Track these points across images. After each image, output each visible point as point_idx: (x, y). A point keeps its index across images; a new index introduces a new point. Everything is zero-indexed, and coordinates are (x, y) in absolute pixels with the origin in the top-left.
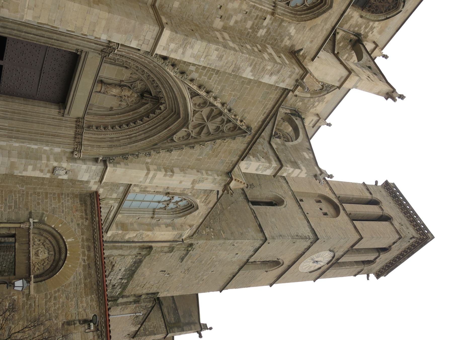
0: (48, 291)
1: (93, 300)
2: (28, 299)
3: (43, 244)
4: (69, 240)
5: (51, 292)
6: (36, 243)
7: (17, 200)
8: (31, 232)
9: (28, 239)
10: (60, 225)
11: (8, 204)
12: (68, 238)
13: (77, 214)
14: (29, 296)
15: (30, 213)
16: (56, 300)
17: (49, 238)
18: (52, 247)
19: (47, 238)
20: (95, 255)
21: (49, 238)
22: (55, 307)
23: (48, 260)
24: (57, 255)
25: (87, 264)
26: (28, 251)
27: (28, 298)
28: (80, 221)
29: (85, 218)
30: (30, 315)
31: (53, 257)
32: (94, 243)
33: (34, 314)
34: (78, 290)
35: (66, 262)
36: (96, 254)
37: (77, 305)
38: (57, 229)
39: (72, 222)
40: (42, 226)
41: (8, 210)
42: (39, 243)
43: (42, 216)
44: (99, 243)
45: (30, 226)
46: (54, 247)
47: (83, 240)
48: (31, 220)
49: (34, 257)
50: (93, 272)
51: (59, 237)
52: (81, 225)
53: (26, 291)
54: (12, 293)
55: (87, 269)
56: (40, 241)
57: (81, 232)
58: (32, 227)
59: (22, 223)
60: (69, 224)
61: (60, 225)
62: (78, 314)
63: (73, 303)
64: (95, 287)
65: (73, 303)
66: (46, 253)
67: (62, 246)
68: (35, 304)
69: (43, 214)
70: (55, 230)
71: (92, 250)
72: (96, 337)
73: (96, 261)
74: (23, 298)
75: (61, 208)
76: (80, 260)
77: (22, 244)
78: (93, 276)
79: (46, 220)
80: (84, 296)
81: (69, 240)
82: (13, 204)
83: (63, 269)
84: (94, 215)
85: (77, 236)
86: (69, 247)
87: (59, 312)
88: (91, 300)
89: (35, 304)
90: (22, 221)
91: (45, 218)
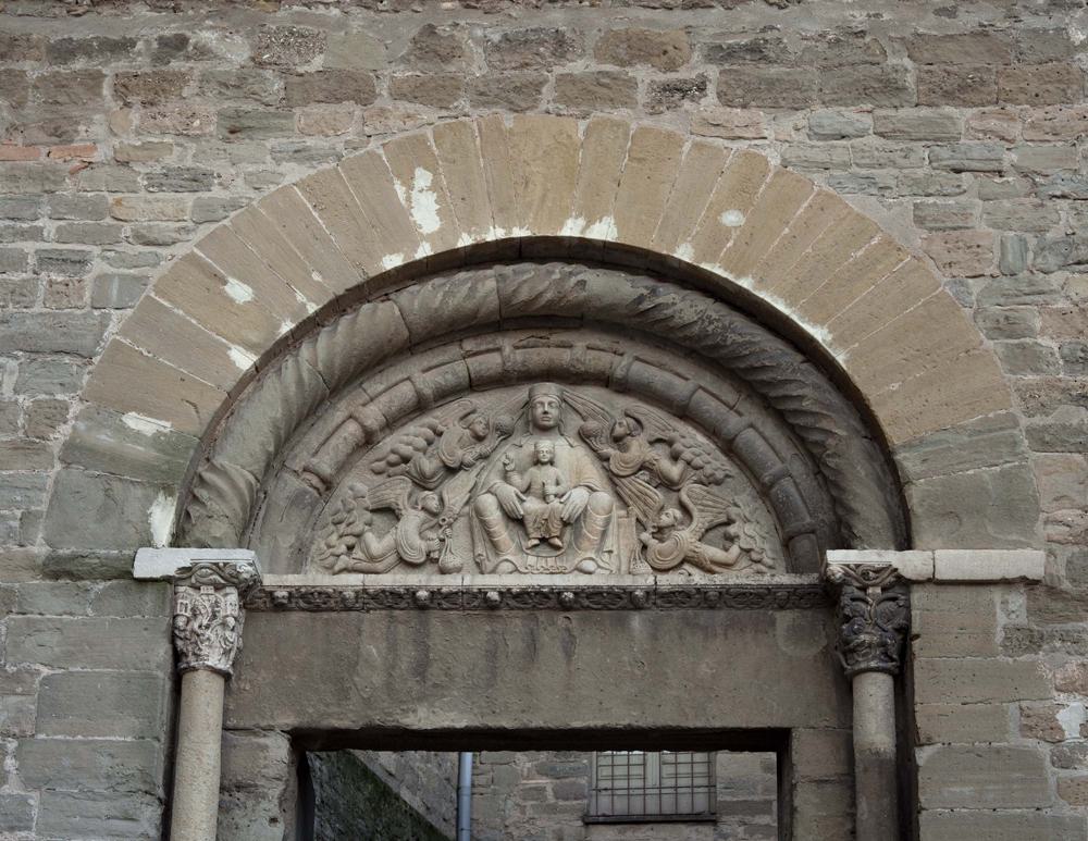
3: (422, 482)
5: (1027, 394)
8: (294, 580)
9: (375, 619)
10: (239, 291)
12: (400, 227)
14: (1052, 591)
15: (58, 570)
17: (373, 415)
19: (368, 440)
24: (581, 350)
25: (713, 72)
26: (515, 625)
28: (198, 104)
31: (590, 395)
35: (684, 253)
38: (287, 327)
39: (197, 180)
40: (240, 457)
45: (226, 577)
46: (476, 385)
48: (156, 562)
49: (586, 557)
51: (379, 319)
53: (1002, 619)
54: (1015, 740)
55: (774, 71)
57: (333, 107)
58: (242, 559)
59: (177, 656)
60: (235, 205)
61: (239, 291)
66: (546, 444)
67: (483, 288)
69: (74, 452)
75: (16, 277)
76: (667, 122)
77: (421, 669)
83: (761, 282)
85: (373, 145)
86: (503, 213)
90: (163, 651)
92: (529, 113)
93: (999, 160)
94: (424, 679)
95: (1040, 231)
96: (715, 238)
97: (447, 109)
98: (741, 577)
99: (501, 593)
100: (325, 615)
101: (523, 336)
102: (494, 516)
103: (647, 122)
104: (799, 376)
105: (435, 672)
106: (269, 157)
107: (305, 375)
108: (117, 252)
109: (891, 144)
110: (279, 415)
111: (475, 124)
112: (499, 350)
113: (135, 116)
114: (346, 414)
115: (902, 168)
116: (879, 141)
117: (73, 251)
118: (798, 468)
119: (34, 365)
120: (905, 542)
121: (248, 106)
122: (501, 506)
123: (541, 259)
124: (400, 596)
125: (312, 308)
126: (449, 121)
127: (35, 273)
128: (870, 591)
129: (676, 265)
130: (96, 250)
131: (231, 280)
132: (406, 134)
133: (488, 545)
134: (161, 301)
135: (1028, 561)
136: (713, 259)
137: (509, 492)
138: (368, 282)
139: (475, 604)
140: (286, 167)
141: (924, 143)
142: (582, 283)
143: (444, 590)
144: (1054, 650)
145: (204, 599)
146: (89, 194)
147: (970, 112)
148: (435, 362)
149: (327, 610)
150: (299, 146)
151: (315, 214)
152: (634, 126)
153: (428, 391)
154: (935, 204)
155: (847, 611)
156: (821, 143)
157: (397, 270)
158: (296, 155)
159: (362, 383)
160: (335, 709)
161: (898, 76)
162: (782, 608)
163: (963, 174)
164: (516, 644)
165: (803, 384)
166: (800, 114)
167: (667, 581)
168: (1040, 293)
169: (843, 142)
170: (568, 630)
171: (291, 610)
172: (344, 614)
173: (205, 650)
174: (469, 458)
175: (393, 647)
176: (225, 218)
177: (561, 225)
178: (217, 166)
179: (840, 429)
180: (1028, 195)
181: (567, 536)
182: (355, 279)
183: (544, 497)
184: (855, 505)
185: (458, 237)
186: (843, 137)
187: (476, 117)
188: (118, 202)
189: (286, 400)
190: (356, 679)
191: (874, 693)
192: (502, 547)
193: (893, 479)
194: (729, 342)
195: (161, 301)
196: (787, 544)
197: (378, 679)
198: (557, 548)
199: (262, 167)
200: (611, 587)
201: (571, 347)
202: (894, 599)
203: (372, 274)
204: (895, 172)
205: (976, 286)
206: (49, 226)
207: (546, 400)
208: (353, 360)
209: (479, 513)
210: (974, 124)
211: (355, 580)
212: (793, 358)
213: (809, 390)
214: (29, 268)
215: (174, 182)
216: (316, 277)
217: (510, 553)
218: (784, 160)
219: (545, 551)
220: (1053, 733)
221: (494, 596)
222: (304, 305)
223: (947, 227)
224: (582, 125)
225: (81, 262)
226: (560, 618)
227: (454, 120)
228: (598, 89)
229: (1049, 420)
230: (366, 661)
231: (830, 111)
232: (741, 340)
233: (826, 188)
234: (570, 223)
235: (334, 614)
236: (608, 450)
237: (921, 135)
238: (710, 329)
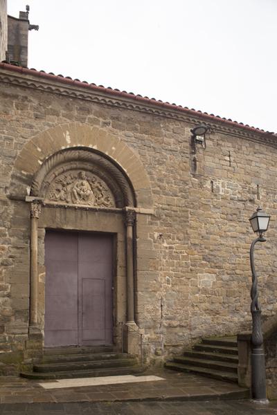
2: (159, 218)
4: (68, 140)
9: (58, 210)
13: (13, 113)
14: (154, 216)
15: (12, 198)
16: (163, 180)
17: (57, 173)
18: (70, 172)
19: (56, 176)
20: (98, 103)
22: (172, 183)
23: (93, 182)
24: (88, 166)
25: (111, 121)
29: (23, 101)
30: (179, 217)
31: (89, 173)
32: (75, 98)
34: (152, 145)
35: (107, 153)
36: (96, 100)
37: (171, 150)
43: (20, 179)
44: (80, 89)
46: (71, 169)
47: (70, 117)
48: (29, 199)
49: (89, 202)
50: (124, 115)
51: (60, 157)
52: (39, 112)
54: (149, 238)
55: (120, 123)
56: (59, 191)
59: (31, 215)
62: (184, 153)
63: (168, 156)
64: (149, 118)
65: (168, 156)
67: (76, 154)
71: (87, 105)
72: (211, 136)
73: (108, 105)
74: (157, 224)
76: (104, 129)
77: (65, 219)
78: (132, 117)
79: (28, 173)
81: (68, 140)
84: (21, 81)
86: (80, 142)
88: (168, 130)
91: (24, 175)
96: (111, 153)
102: (76, 194)
113: (20, 111)
118: (119, 190)
120: (135, 206)
121: (39, 113)
135: (151, 211)
140: (46, 127)
145: (36, 205)
147: (147, 136)
164: (79, 216)
167: (102, 207)
175: (61, 214)
178: (34, 124)
179: (127, 186)
187: (76, 122)
191: (130, 229)
193: (134, 196)
196: (116, 203)
209: (73, 192)
211: (55, 203)
212: (120, 173)
213: (123, 179)
217: (78, 200)
220: (152, 236)
225: (12, 140)
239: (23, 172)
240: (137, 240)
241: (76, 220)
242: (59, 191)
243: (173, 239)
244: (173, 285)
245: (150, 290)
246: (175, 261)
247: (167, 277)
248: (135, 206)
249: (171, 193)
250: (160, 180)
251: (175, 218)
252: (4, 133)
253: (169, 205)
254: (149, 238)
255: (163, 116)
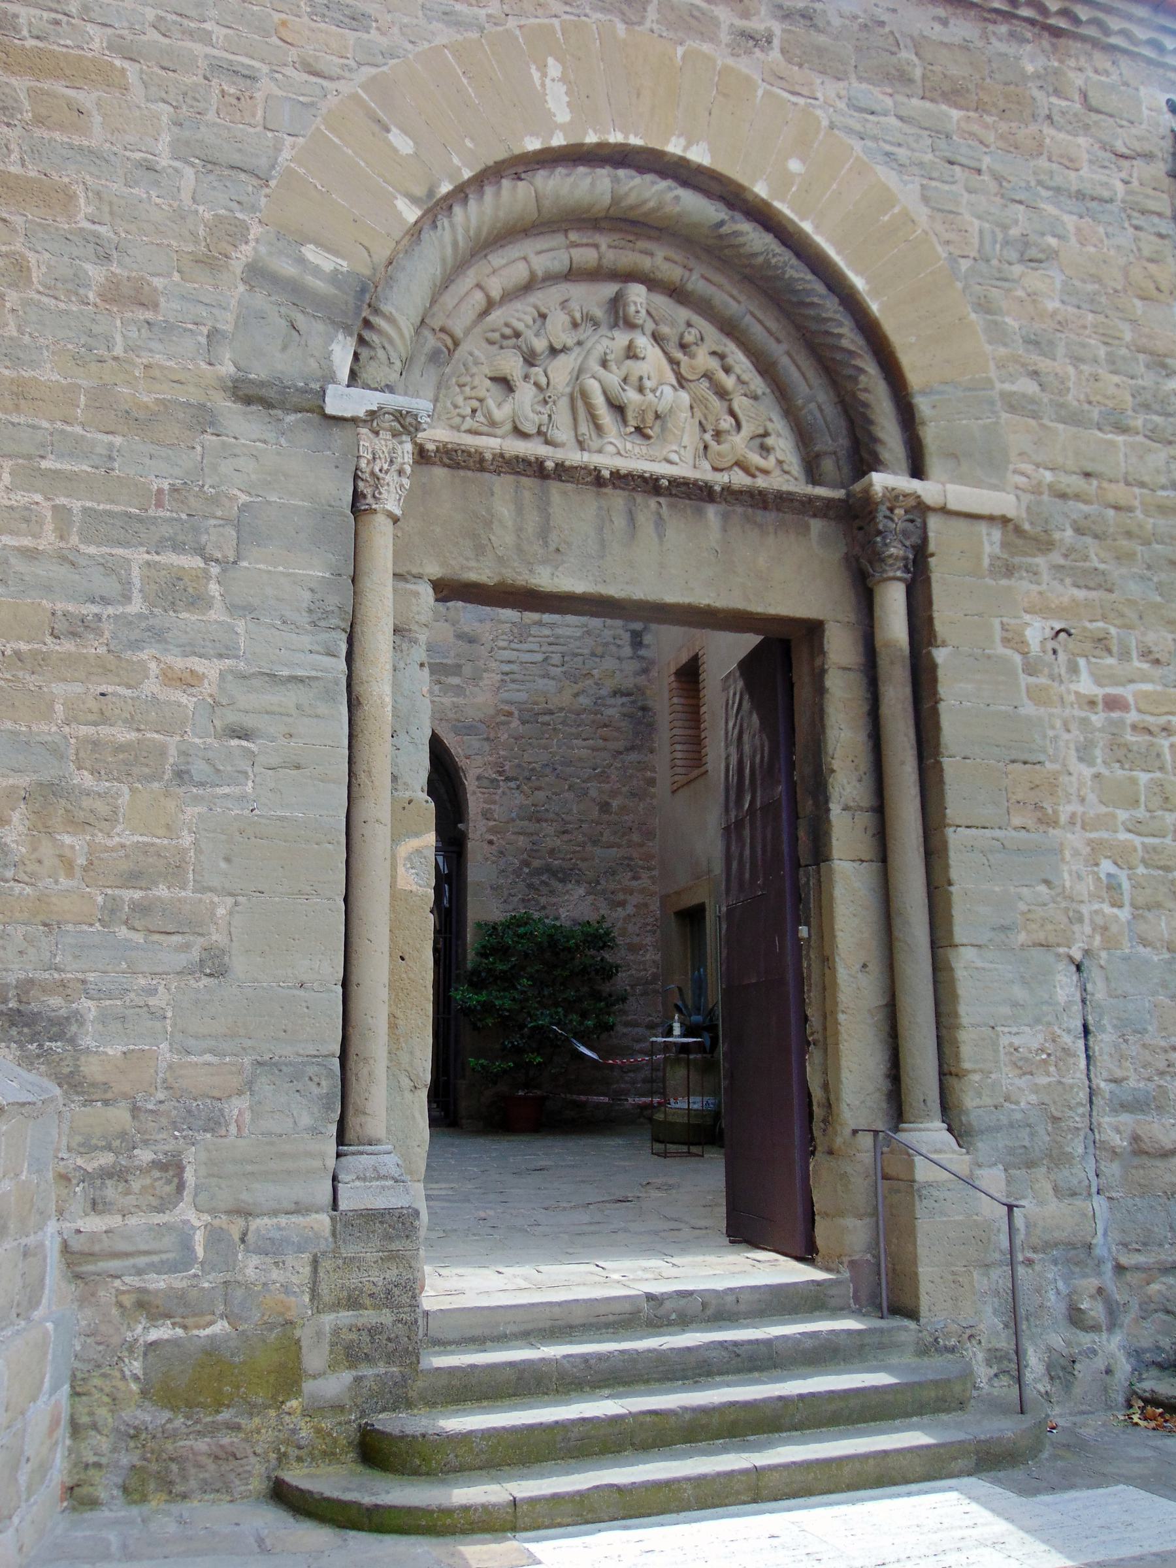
0: (989, 381)
1: (1056, 72)
2: (1044, 544)
6: (531, 415)
7: (76, 505)
10: (402, 144)
11: (136, 606)
14: (1018, 531)
21: (496, 294)
25: (777, 27)
26: (617, 499)
27: (1036, 539)
30: (1146, 543)
31: (661, 301)
33: (1139, 514)
35: (761, 190)
37: (1080, 196)
38: (445, 188)
41: (217, 614)
42: (526, 394)
43: (295, 292)
46: (573, 274)
49: (670, 449)
55: (822, 39)
61: (402, 144)
65: (1070, 221)
68: (1077, 497)
70: (446, 204)
76: (744, 65)
77: (544, 533)
80: (1033, 128)
82: (139, 556)
83: (817, 227)
85: (512, 23)
87: (1128, 336)
88: (1057, 92)
89: (1077, 497)
91: (316, 271)
92: (637, 28)
93: (979, 160)
94: (546, 545)
95: (1005, 228)
97: (571, 5)
98: (776, 482)
99: (612, 473)
100: (462, 473)
101: (616, 236)
102: (599, 401)
103: (730, 61)
104: (838, 316)
105: (554, 537)
106: (420, 13)
107: (460, 238)
108: (284, 75)
109: (906, 128)
110: (438, 273)
111: (594, 27)
112: (596, 246)
114: (475, 282)
115: (913, 150)
116: (898, 123)
117: (243, 65)
119: (211, 177)
122: (605, 393)
123: (641, 170)
124: (529, 463)
125: (467, 174)
126: (573, 18)
127: (206, 78)
128: (897, 511)
129: (750, 198)
130: (265, 69)
131: (394, 130)
132: (538, 21)
133: (592, 426)
134: (331, 136)
136: (783, 201)
137: (613, 379)
138: (511, 158)
139: (589, 479)
140: (437, 26)
141: (928, 133)
142: (677, 198)
143: (567, 463)
144: (1021, 578)
146: (255, 8)
148: (546, 246)
149: (463, 468)
150: (448, 9)
151: (465, 81)
152: (719, 62)
153: (540, 274)
154: (936, 188)
155: (881, 527)
156: (856, 114)
157: (537, 153)
158: (445, 17)
159: (486, 256)
160: (473, 564)
161: (910, 68)
162: (815, 516)
163: (955, 167)
164: (620, 522)
165: (841, 325)
166: (841, 84)
167: (739, 479)
168: (1006, 280)
169: (871, 117)
170: (659, 514)
171: (434, 464)
172: (479, 474)
173: (385, 495)
174: (570, 342)
175: (520, 510)
176: (385, 64)
177: (667, 141)
180: (996, 195)
181: (657, 428)
182: (501, 155)
183: (641, 390)
184: (881, 435)
185: (586, 133)
186: (873, 113)
188: (284, 23)
189: (443, 260)
190: (493, 538)
192: (606, 429)
194: (787, 276)
195: (331, 136)
197: (510, 539)
198: (648, 437)
199: (415, 21)
200: (696, 480)
201: (652, 255)
202: (912, 521)
203: (517, 151)
204: (909, 153)
205: (965, 265)
206: (219, 33)
207: (639, 300)
208: (495, 232)
209: (584, 395)
210: (963, 125)
214: (200, 72)
215: (335, 15)
216: (469, 144)
218: (831, 122)
219: (638, 440)
221: (606, 474)
222: (460, 169)
223: (946, 213)
224: (680, 51)
226: (652, 502)
227: (576, 18)
228: (689, 19)
229: (1014, 388)
230: (500, 521)
231: (864, 86)
232: (796, 275)
233: (861, 154)
234: (674, 139)
235: (469, 473)
236: (678, 355)
237: (927, 125)
238: (773, 261)
239: (311, 253)
240: (941, 655)
241: (602, 544)
242: (505, 383)
243: (1125, 656)
244: (1140, 910)
245: (1022, 937)
246: (1143, 777)
247: (1106, 866)
248: (917, 471)
249: (1095, 415)
250: (1033, 342)
251: (1124, 543)
252: (206, 38)
253: (1087, 475)
254: (1001, 650)
255: (1032, 22)
